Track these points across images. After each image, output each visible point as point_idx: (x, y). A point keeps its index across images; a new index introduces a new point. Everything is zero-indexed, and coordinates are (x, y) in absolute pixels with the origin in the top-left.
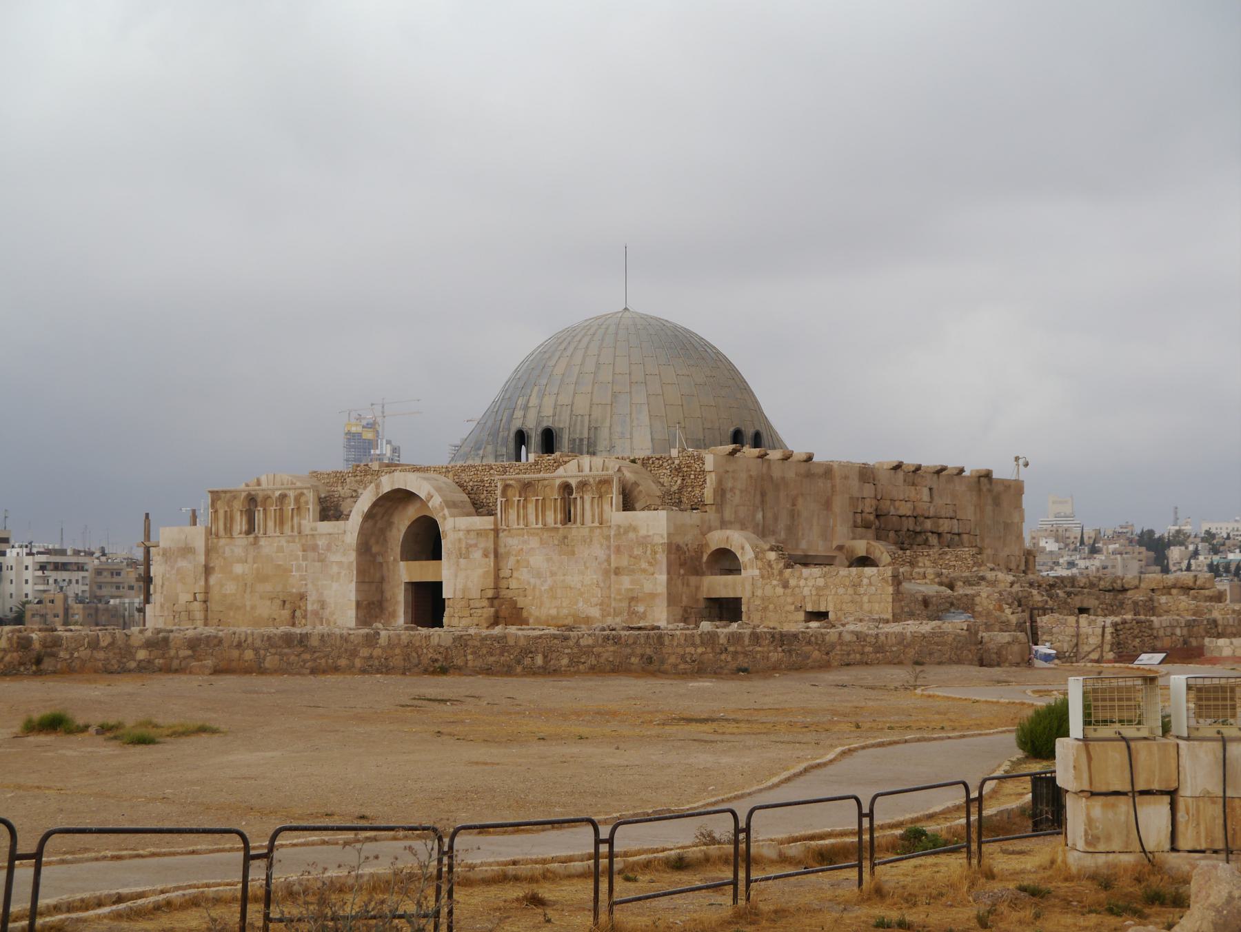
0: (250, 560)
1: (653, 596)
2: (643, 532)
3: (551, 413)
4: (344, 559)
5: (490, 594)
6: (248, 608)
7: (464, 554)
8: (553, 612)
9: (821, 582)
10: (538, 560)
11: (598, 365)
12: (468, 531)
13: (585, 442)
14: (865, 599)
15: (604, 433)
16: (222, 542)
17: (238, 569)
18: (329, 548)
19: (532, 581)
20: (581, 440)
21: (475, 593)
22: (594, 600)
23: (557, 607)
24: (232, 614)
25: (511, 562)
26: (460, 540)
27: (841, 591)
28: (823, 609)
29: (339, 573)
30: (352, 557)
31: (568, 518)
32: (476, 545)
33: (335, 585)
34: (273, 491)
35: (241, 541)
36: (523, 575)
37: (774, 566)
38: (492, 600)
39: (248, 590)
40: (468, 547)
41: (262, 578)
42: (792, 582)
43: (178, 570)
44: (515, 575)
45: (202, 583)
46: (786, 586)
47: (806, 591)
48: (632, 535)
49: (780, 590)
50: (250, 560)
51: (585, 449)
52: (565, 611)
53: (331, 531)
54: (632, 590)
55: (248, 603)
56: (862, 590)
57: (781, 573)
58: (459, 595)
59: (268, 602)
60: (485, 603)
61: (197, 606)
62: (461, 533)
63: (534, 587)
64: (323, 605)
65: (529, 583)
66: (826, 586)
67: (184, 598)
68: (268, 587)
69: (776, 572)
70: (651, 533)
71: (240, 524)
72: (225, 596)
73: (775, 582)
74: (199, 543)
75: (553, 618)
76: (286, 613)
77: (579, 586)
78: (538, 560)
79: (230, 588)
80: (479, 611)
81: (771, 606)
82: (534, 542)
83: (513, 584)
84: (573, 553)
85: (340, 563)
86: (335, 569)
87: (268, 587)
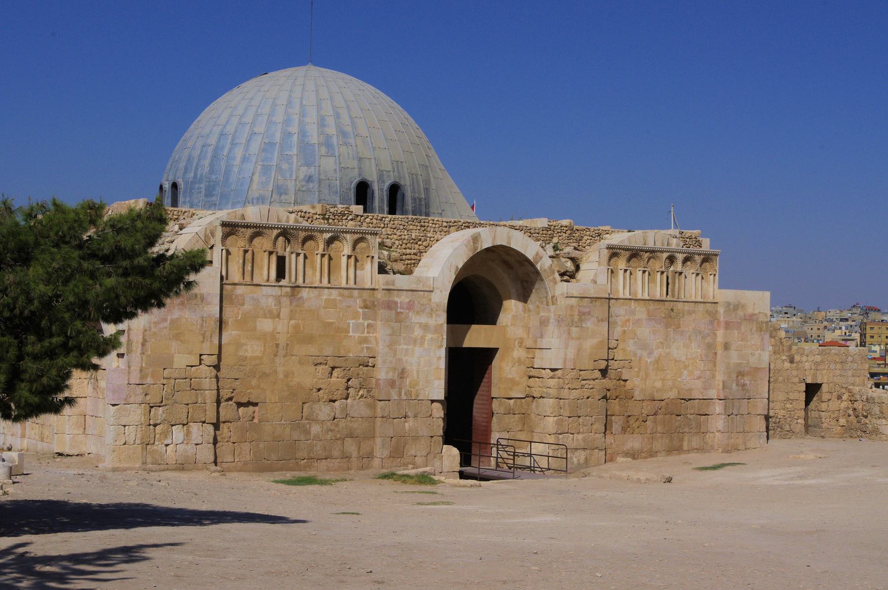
0: (285, 312)
1: (757, 369)
2: (750, 311)
3: (390, 168)
4: (432, 322)
6: (281, 376)
8: (658, 384)
9: (818, 358)
11: (257, 115)
13: (423, 203)
14: (850, 373)
15: (433, 194)
16: (240, 290)
17: (266, 325)
18: (410, 306)
19: (639, 352)
20: (420, 200)
21: (587, 364)
22: (697, 373)
23: (663, 380)
24: (254, 382)
25: (617, 332)
26: (572, 307)
27: (832, 366)
28: (819, 382)
29: (423, 338)
30: (443, 318)
32: (589, 313)
33: (418, 350)
34: (322, 232)
36: (631, 346)
37: (785, 344)
38: (604, 372)
39: (281, 352)
40: (582, 314)
41: (300, 337)
42: (797, 358)
43: (173, 322)
44: (620, 346)
45: (224, 341)
46: (792, 361)
47: (807, 365)
48: (740, 313)
49: (787, 365)
50: (285, 312)
51: (424, 210)
52: (670, 383)
53: (414, 287)
54: (739, 364)
55: (280, 369)
56: (847, 366)
57: (790, 348)
58: (570, 365)
59: (312, 368)
60: (598, 374)
61: (206, 371)
62: (574, 301)
63: (640, 358)
64: (403, 374)
65: (635, 355)
66: (822, 362)
67: (181, 360)
68: (312, 350)
69: (785, 348)
70: (756, 312)
72: (245, 359)
73: (784, 358)
75: (658, 390)
77: (683, 358)
78: (645, 332)
79: (253, 349)
80: (592, 382)
81: (780, 379)
82: (641, 312)
84: (678, 326)
85: (425, 327)
86: (418, 332)
87: (312, 350)
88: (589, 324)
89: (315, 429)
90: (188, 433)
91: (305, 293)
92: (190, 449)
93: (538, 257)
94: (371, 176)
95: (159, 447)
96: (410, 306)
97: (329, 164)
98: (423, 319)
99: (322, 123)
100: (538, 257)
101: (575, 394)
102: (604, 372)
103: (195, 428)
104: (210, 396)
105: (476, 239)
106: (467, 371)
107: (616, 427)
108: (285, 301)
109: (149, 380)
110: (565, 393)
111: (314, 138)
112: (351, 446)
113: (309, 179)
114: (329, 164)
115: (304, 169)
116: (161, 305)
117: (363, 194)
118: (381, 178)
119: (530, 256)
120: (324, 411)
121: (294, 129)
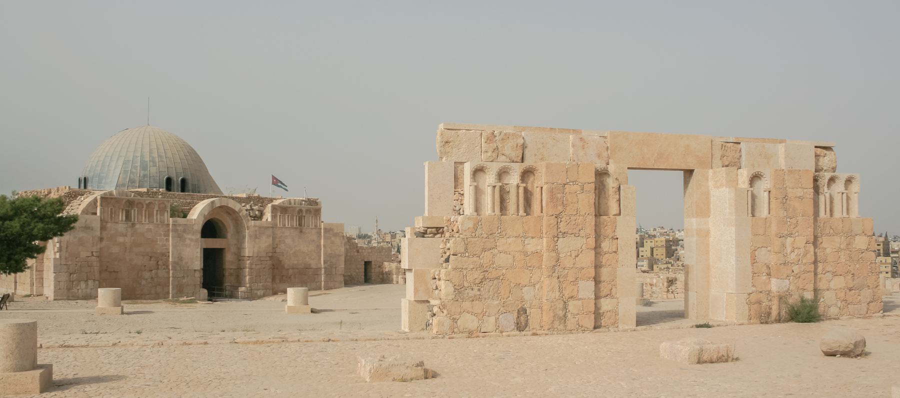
4: (193, 237)
5: (270, 254)
7: (255, 237)
10: (288, 241)
12: (260, 227)
18: (184, 231)
25: (277, 240)
31: (300, 225)
33: (188, 249)
35: (122, 227)
36: (282, 246)
38: (271, 257)
67: (84, 254)
71: (122, 216)
74: (97, 225)
76: (153, 262)
79: (115, 250)
82: (287, 233)
83: (278, 250)
85: (191, 240)
86: (188, 242)
88: (264, 238)
89: (143, 282)
90: (87, 285)
91: (137, 226)
92: (88, 291)
93: (241, 210)
94: (173, 175)
95: (75, 290)
96: (184, 231)
97: (153, 170)
98: (189, 236)
99: (151, 152)
100: (241, 210)
101: (258, 267)
102: (271, 257)
103: (90, 282)
104: (96, 269)
105: (213, 202)
106: (212, 258)
107: (277, 281)
108: (129, 230)
109: (70, 263)
110: (254, 266)
111: (147, 159)
112: (159, 289)
113: (144, 176)
114: (153, 170)
115: (142, 172)
116: (61, 235)
117: (169, 182)
118: (178, 177)
119: (237, 210)
120: (147, 275)
121: (139, 154)
